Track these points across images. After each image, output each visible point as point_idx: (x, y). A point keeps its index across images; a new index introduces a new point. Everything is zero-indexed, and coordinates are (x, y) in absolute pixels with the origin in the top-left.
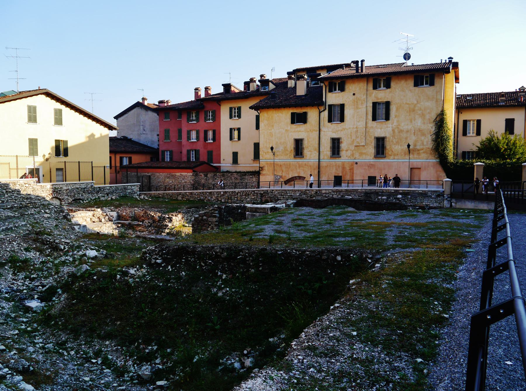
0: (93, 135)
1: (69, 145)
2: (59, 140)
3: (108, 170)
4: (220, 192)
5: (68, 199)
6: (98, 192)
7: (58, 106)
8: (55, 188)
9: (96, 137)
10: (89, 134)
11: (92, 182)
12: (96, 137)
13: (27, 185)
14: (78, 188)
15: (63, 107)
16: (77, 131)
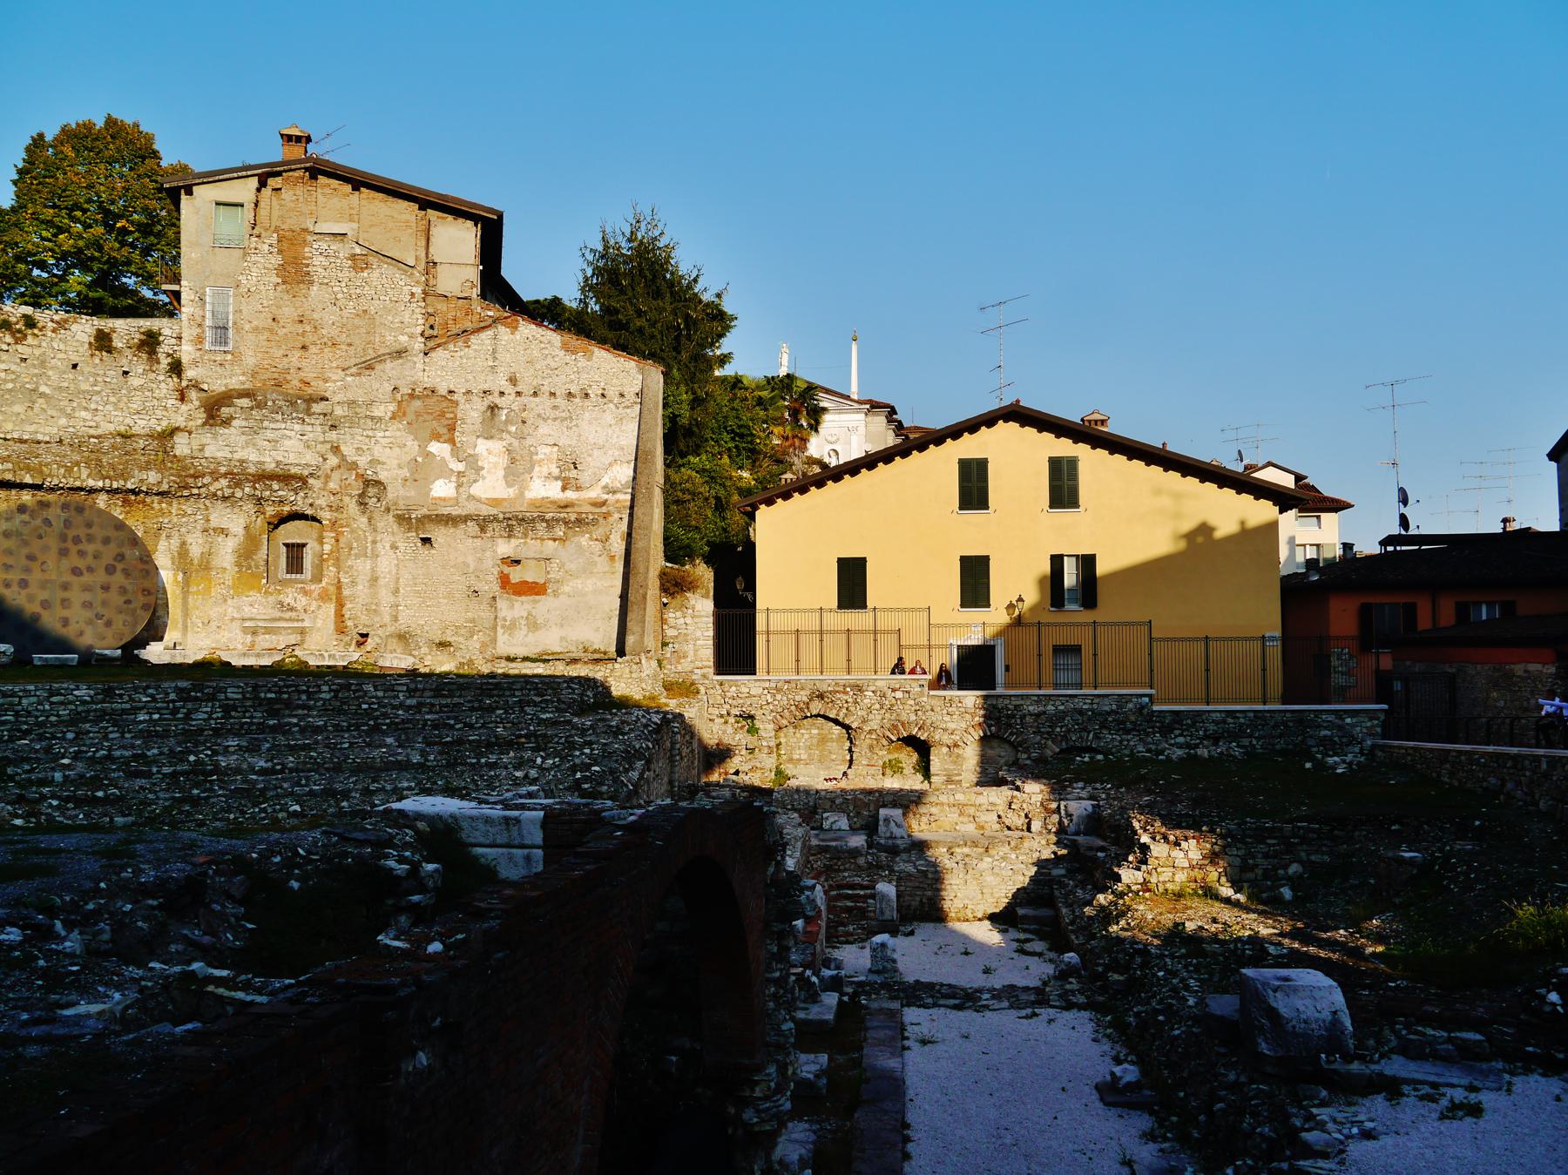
0: (1205, 529)
1: (1102, 568)
2: (1061, 557)
3: (1275, 652)
4: (1537, 758)
5: (1043, 747)
6: (1166, 731)
7: (1065, 447)
8: (994, 706)
9: (1219, 534)
10: (1188, 525)
11: (1148, 691)
12: (1219, 534)
13: (899, 695)
14: (1081, 712)
15: (1082, 451)
16: (1131, 520)
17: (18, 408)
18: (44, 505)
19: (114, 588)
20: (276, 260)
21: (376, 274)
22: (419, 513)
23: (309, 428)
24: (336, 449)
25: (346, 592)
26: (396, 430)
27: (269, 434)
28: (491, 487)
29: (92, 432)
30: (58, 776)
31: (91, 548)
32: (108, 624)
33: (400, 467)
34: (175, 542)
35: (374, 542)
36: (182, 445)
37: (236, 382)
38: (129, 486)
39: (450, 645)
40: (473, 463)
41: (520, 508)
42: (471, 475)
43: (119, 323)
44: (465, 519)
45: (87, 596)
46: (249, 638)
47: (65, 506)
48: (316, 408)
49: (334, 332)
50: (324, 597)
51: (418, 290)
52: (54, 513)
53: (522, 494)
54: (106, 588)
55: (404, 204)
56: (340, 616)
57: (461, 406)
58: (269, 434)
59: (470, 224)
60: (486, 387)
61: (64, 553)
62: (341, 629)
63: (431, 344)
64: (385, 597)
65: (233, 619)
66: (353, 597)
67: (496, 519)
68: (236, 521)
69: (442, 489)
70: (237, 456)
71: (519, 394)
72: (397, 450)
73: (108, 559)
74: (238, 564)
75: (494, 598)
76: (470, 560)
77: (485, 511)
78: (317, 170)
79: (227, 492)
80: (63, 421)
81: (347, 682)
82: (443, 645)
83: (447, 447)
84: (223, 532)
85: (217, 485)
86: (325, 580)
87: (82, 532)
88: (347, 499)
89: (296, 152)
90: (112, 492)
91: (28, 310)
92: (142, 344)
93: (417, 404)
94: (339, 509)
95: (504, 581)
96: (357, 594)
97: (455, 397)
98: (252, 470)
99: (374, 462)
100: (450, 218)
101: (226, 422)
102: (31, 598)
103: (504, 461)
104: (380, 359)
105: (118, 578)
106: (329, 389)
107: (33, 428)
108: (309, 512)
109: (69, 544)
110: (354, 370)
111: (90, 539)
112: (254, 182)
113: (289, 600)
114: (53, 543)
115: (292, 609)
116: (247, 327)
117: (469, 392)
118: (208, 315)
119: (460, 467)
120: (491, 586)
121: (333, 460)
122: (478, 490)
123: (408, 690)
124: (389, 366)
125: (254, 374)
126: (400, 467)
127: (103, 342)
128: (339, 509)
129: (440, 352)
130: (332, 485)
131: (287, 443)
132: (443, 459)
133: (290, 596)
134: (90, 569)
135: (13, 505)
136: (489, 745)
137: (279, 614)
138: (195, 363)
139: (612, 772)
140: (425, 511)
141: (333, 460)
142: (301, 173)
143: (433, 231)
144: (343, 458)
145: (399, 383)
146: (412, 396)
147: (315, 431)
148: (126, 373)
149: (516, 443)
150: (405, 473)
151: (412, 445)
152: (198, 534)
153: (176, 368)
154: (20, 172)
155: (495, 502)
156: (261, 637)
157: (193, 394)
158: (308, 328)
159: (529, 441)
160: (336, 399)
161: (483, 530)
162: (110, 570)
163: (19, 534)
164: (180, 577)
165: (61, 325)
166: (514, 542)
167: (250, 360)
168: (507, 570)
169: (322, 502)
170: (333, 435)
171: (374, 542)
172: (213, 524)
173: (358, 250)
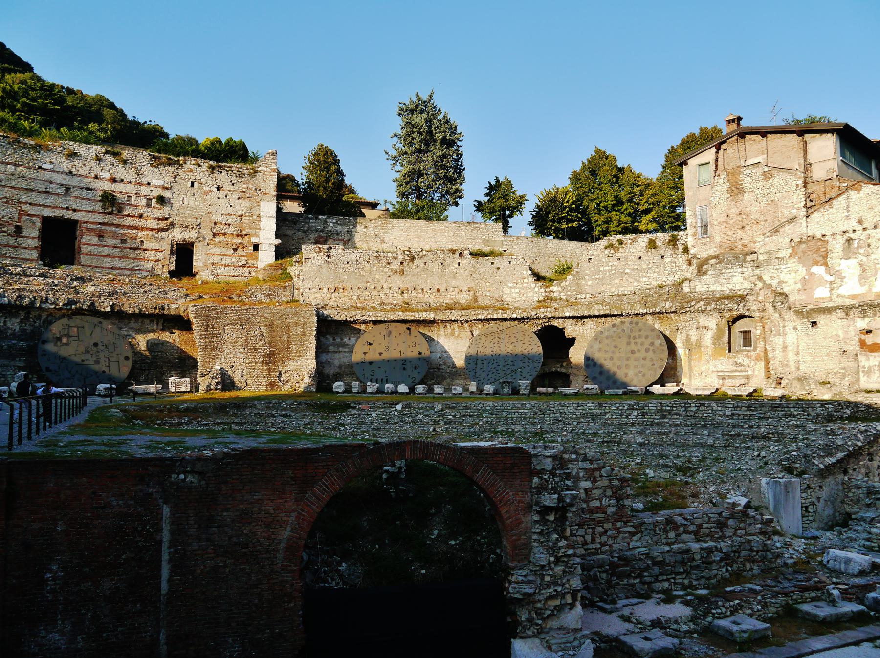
17: (617, 281)
18: (623, 323)
19: (648, 359)
20: (727, 186)
21: (777, 180)
22: (808, 308)
23: (745, 269)
24: (760, 279)
25: (770, 355)
26: (793, 263)
27: (726, 276)
28: (852, 288)
29: (648, 287)
30: (559, 439)
31: (639, 341)
32: (644, 375)
33: (796, 283)
34: (684, 335)
35: (784, 327)
36: (686, 288)
37: (712, 252)
38: (657, 310)
39: (829, 383)
40: (839, 275)
41: (870, 298)
42: (838, 282)
43: (659, 235)
44: (835, 309)
45: (636, 363)
46: (721, 381)
47: (631, 323)
48: (749, 258)
49: (757, 216)
50: (758, 358)
51: (800, 182)
52: (627, 325)
53: (870, 290)
54: (644, 359)
55: (791, 136)
56: (767, 368)
57: (830, 243)
58: (726, 276)
59: (830, 135)
60: (844, 229)
61: (628, 344)
62: (768, 376)
63: (810, 211)
64: (791, 356)
65: (713, 372)
66: (774, 358)
67: (853, 307)
68: (712, 322)
69: (821, 293)
70: (711, 289)
71: (864, 229)
72: (793, 274)
73: (646, 346)
74: (714, 344)
75: (857, 355)
76: (841, 333)
77: (848, 302)
78: (742, 135)
79: (703, 308)
80: (635, 284)
81: (783, 406)
82: (825, 383)
83: (823, 268)
84: (706, 328)
85: (698, 305)
86: (758, 350)
87: (637, 334)
88: (767, 305)
89: (734, 126)
90: (652, 313)
91: (619, 237)
92: (670, 241)
93: (804, 246)
94: (764, 310)
95: (863, 344)
96: (777, 356)
97: (826, 238)
98: (718, 295)
99: (781, 283)
100: (818, 135)
101: (705, 273)
102: (614, 364)
103: (858, 271)
104: (782, 225)
105: (650, 354)
106: (757, 247)
107: (623, 289)
108: (747, 314)
109: (631, 340)
110: (769, 234)
111: (640, 336)
112: (714, 150)
113: (740, 361)
114: (624, 340)
115: (742, 366)
116: (716, 223)
117: (834, 234)
118: (699, 221)
119: (832, 278)
120: (853, 347)
121: (760, 285)
122: (842, 291)
123: (734, 407)
124: (788, 229)
125: (720, 246)
126: (796, 283)
127: (652, 244)
128: (764, 310)
129: (816, 214)
130: (761, 298)
131: (734, 279)
132: (820, 275)
133: (740, 358)
134: (639, 351)
135: (611, 324)
136: (753, 437)
137: (735, 368)
138: (694, 246)
139: (805, 456)
140: (811, 307)
141: (760, 285)
142: (735, 137)
143: (809, 146)
144: (764, 282)
145: (793, 237)
146: (800, 242)
147: (748, 270)
148: (663, 257)
149: (865, 259)
150: (799, 286)
151: (802, 271)
152: (694, 330)
153: (686, 250)
154: (664, 167)
155: (854, 297)
156: (727, 381)
157: (694, 261)
158: (744, 217)
159: (873, 257)
160: (761, 251)
161: (847, 314)
162: (647, 350)
163: (612, 337)
164: (687, 351)
165: (634, 241)
166: (867, 320)
167: (718, 239)
168: (863, 337)
169: (754, 308)
170: (758, 271)
171: (784, 327)
172: (702, 323)
173: (766, 169)
